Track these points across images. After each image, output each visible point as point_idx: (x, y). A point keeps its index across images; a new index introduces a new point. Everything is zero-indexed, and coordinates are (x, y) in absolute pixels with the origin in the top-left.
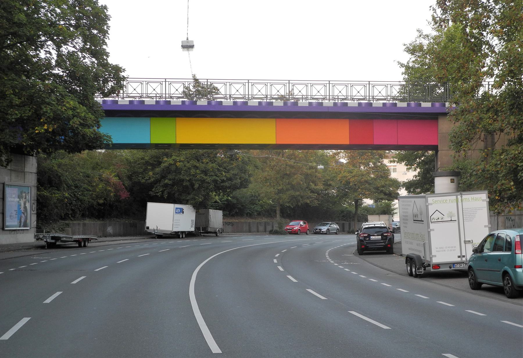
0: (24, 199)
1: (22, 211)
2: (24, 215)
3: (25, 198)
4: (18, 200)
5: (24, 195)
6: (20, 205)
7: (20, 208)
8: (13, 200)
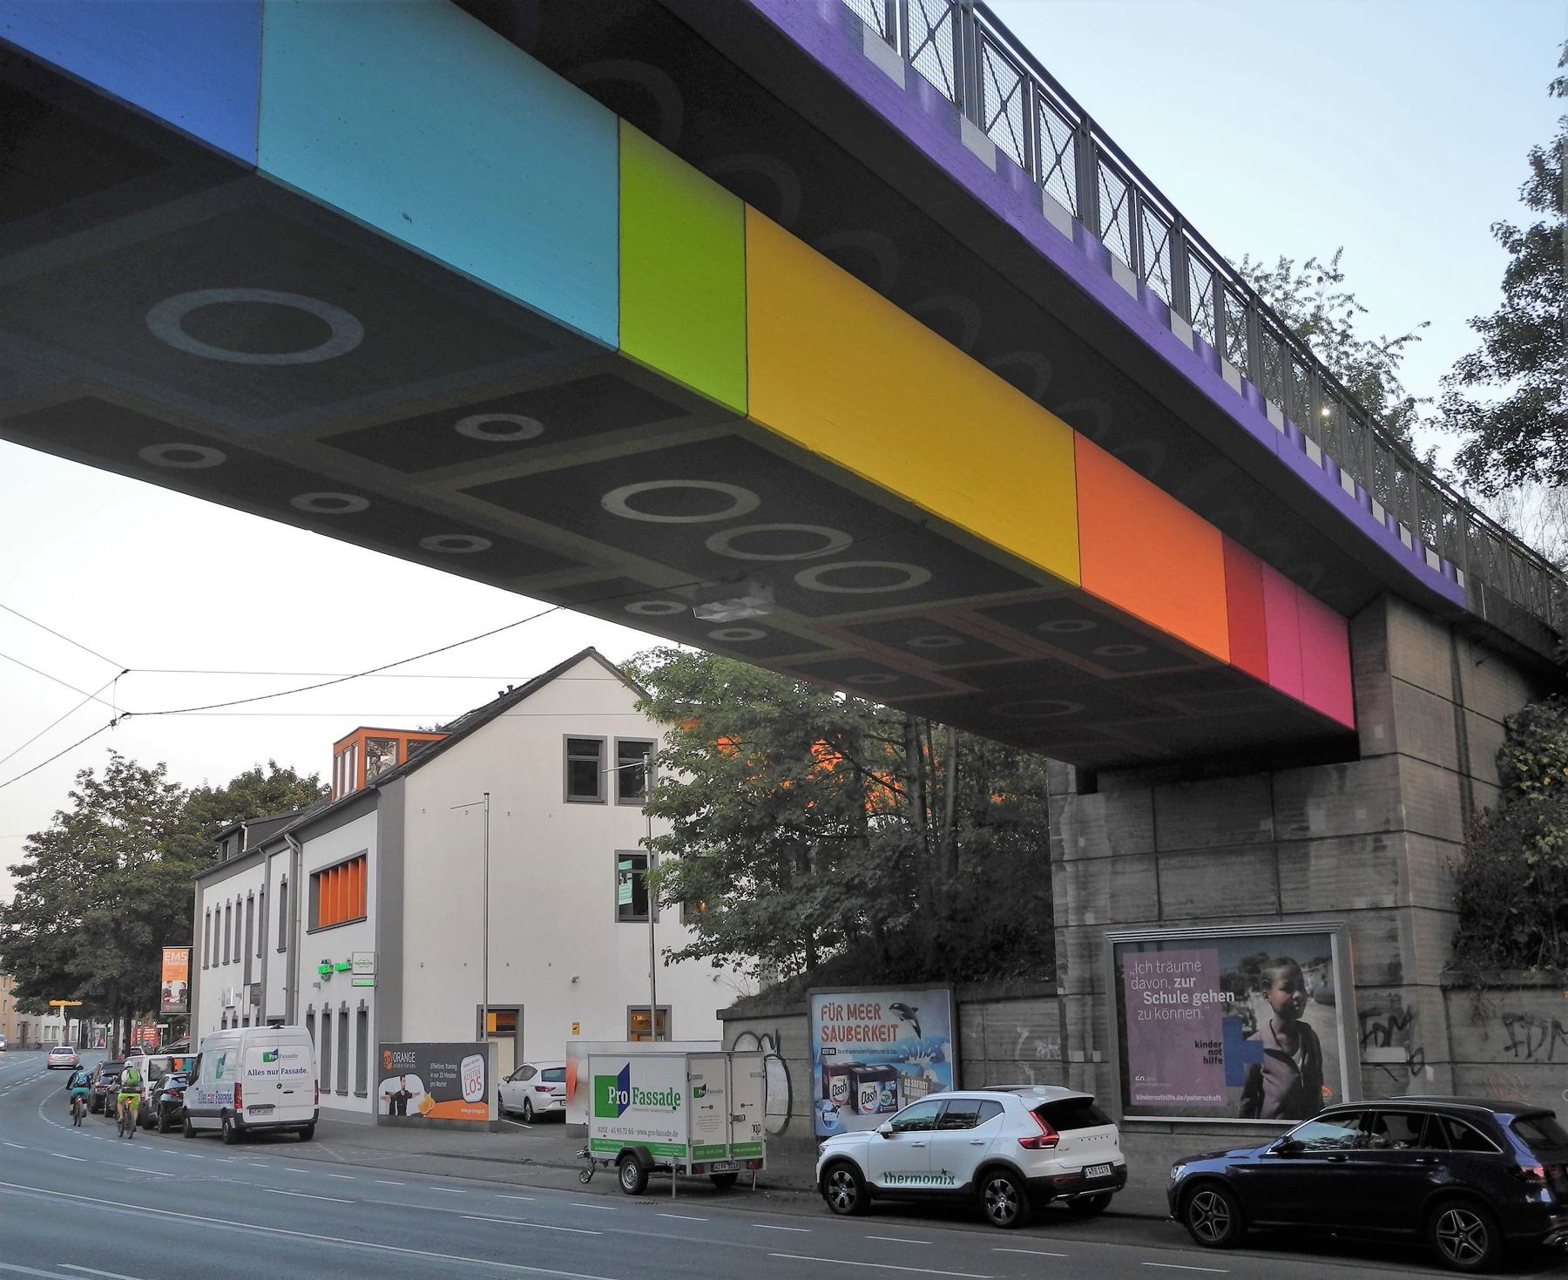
0: (1279, 995)
1: (1270, 1044)
2: (1293, 1065)
3: (1294, 982)
4: (1220, 997)
5: (1278, 973)
6: (1250, 1018)
7: (1249, 1034)
8: (1185, 998)
